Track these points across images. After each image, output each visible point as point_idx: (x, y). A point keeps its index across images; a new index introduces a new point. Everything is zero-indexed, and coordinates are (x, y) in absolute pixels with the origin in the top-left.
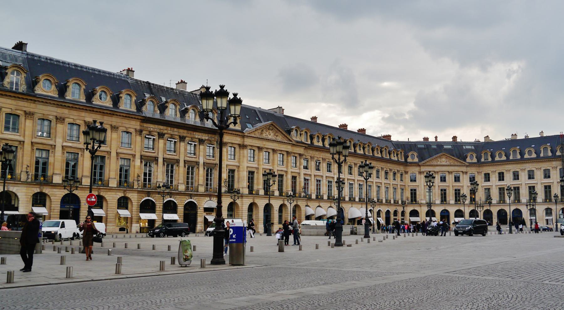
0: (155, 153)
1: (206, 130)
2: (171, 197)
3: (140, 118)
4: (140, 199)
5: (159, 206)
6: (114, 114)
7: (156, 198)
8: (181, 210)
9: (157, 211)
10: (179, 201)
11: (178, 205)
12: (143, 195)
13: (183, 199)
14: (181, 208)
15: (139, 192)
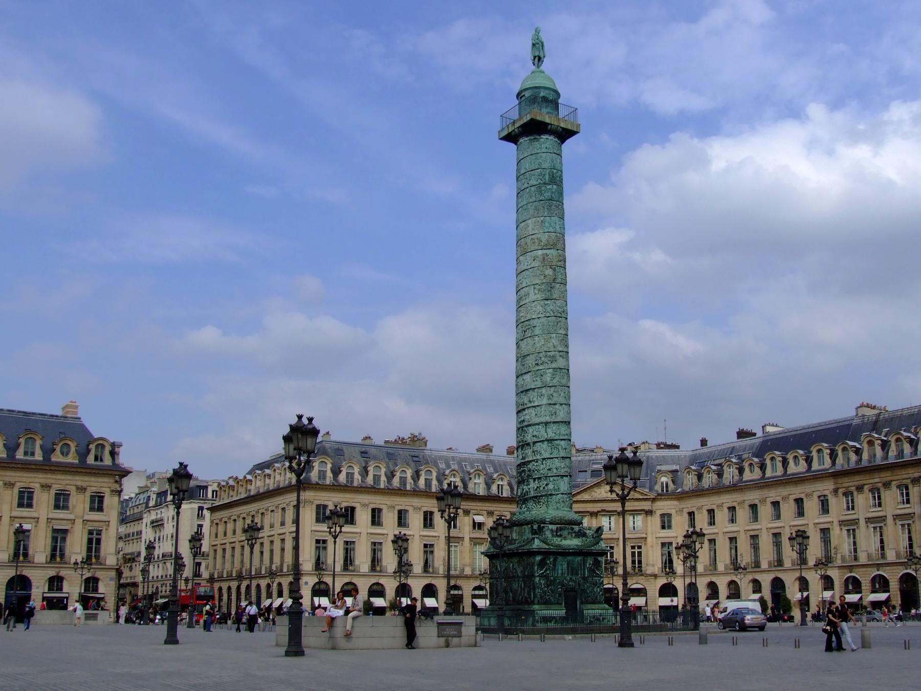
0: (855, 513)
1: (912, 464)
2: (878, 571)
3: (827, 475)
4: (842, 577)
5: (866, 585)
6: (804, 480)
7: (861, 573)
8: (894, 587)
9: (863, 591)
10: (891, 574)
11: (890, 581)
12: (844, 571)
13: (894, 571)
14: (893, 584)
15: (840, 567)
